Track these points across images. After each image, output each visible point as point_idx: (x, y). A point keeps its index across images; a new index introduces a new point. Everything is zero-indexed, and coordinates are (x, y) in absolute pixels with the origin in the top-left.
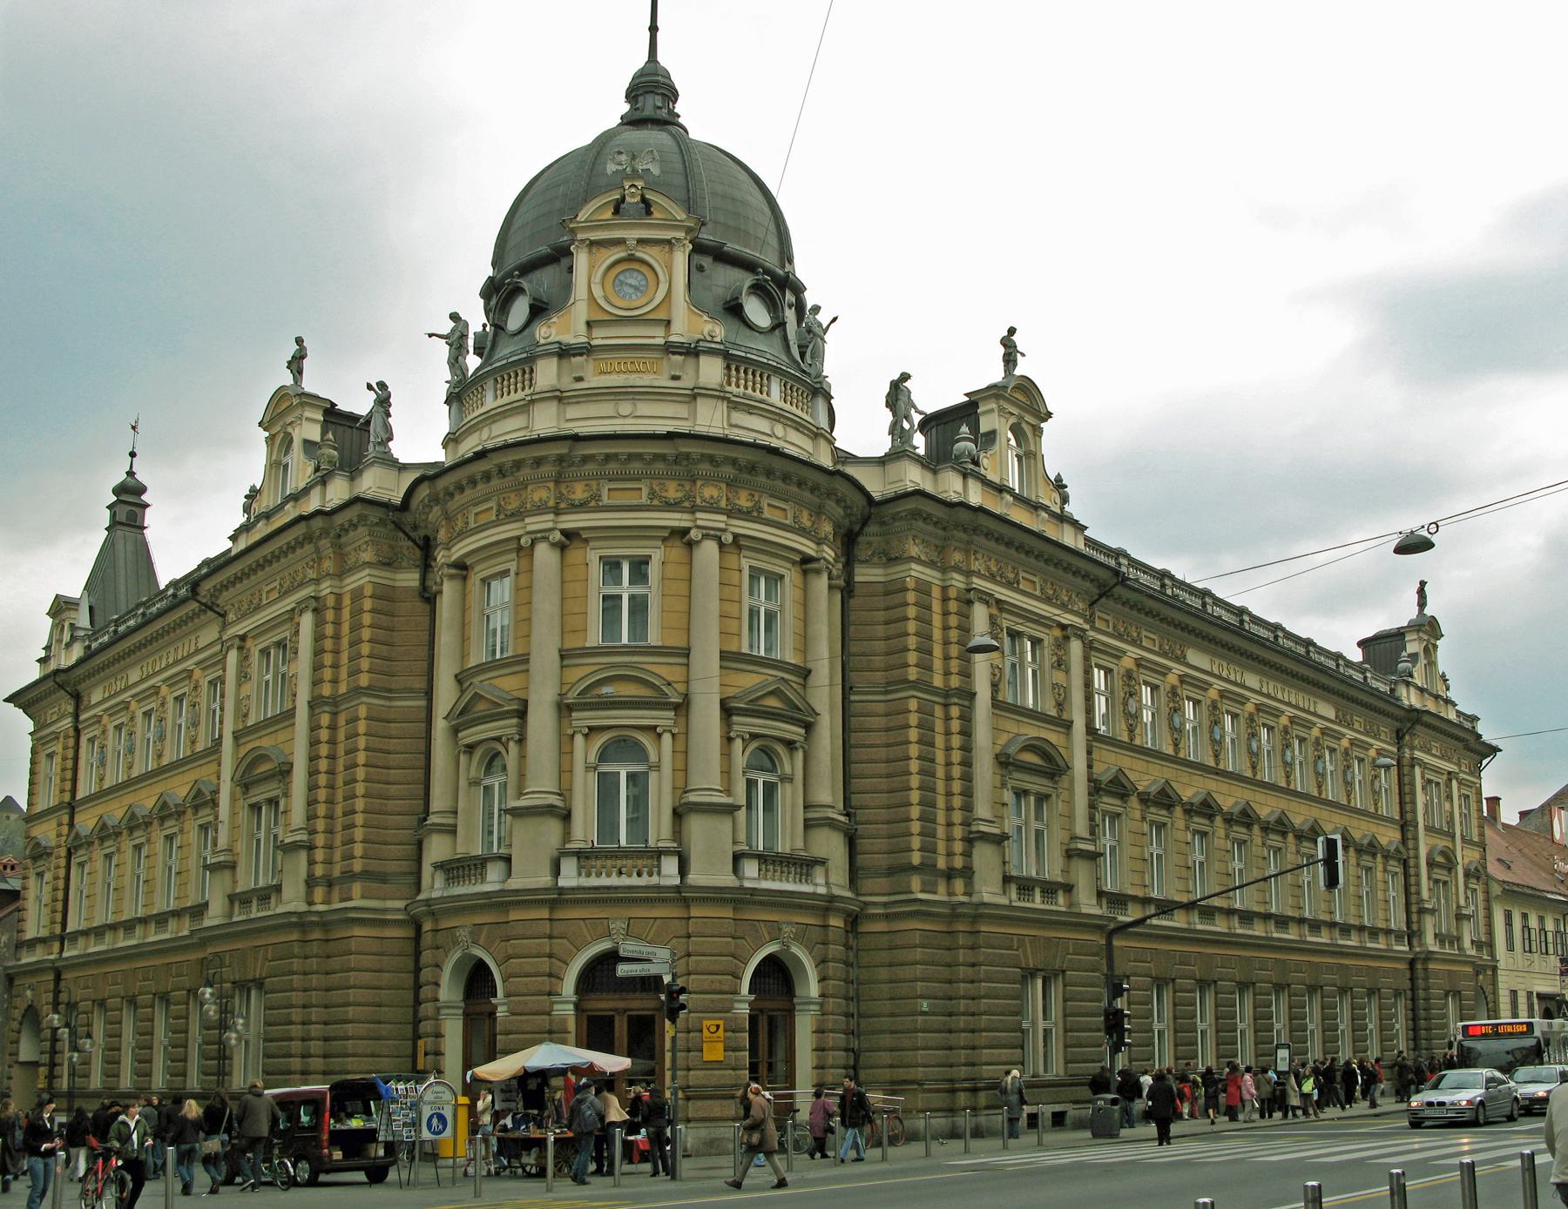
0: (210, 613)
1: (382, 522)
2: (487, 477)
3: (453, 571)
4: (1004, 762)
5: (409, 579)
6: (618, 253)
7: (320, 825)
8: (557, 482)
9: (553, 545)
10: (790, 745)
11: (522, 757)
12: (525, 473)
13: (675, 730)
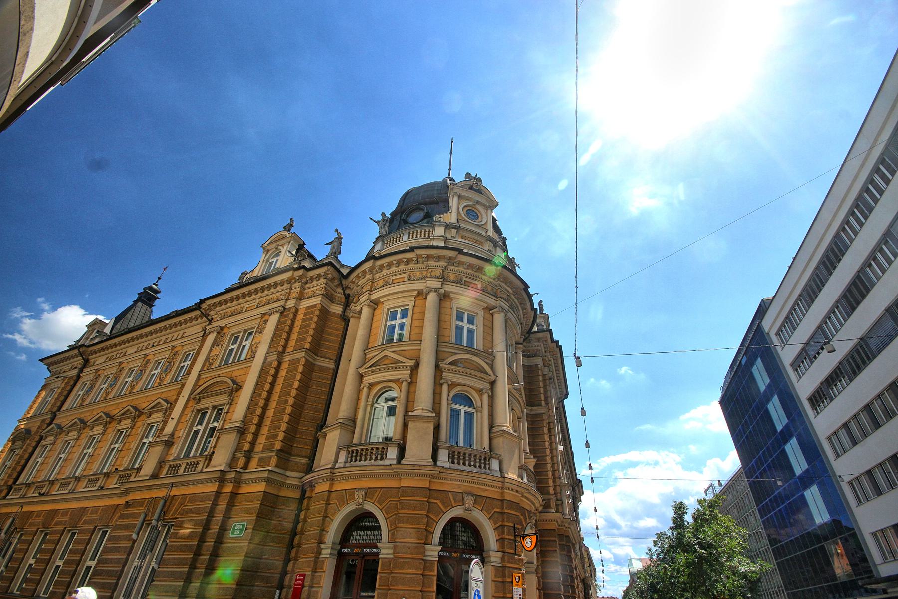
0: (204, 319)
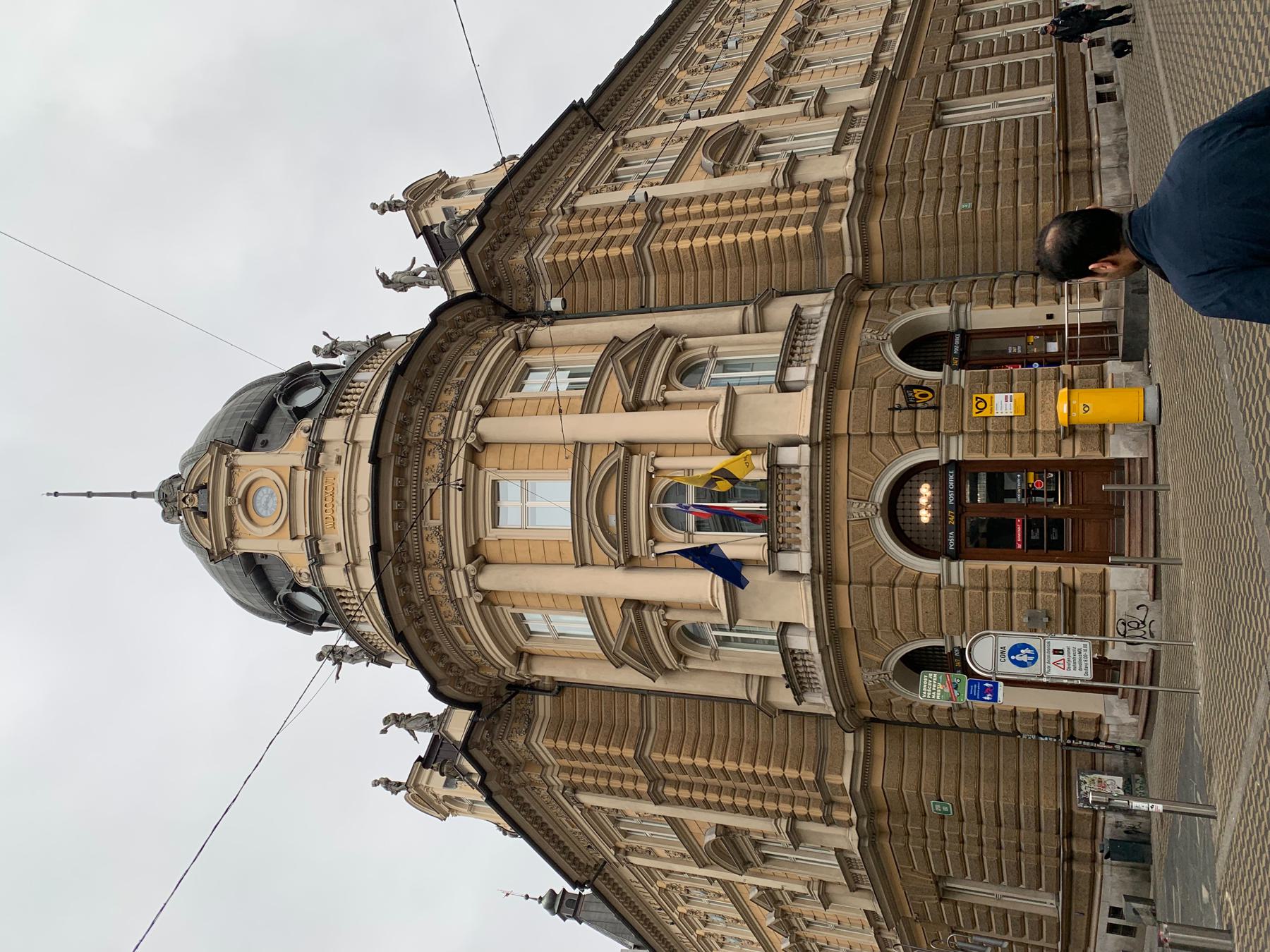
1: (490, 729)
2: (425, 631)
3: (523, 666)
4: (722, 170)
5: (544, 704)
6: (239, 510)
9: (480, 570)
10: (679, 350)
11: (682, 607)
13: (652, 454)
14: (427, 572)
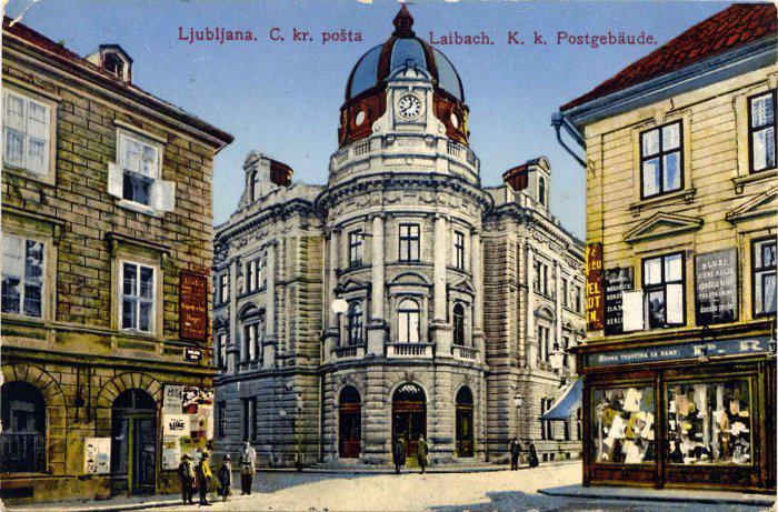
7: (280, 334)
8: (384, 191)
10: (467, 303)
12: (370, 187)
14: (380, 193)
